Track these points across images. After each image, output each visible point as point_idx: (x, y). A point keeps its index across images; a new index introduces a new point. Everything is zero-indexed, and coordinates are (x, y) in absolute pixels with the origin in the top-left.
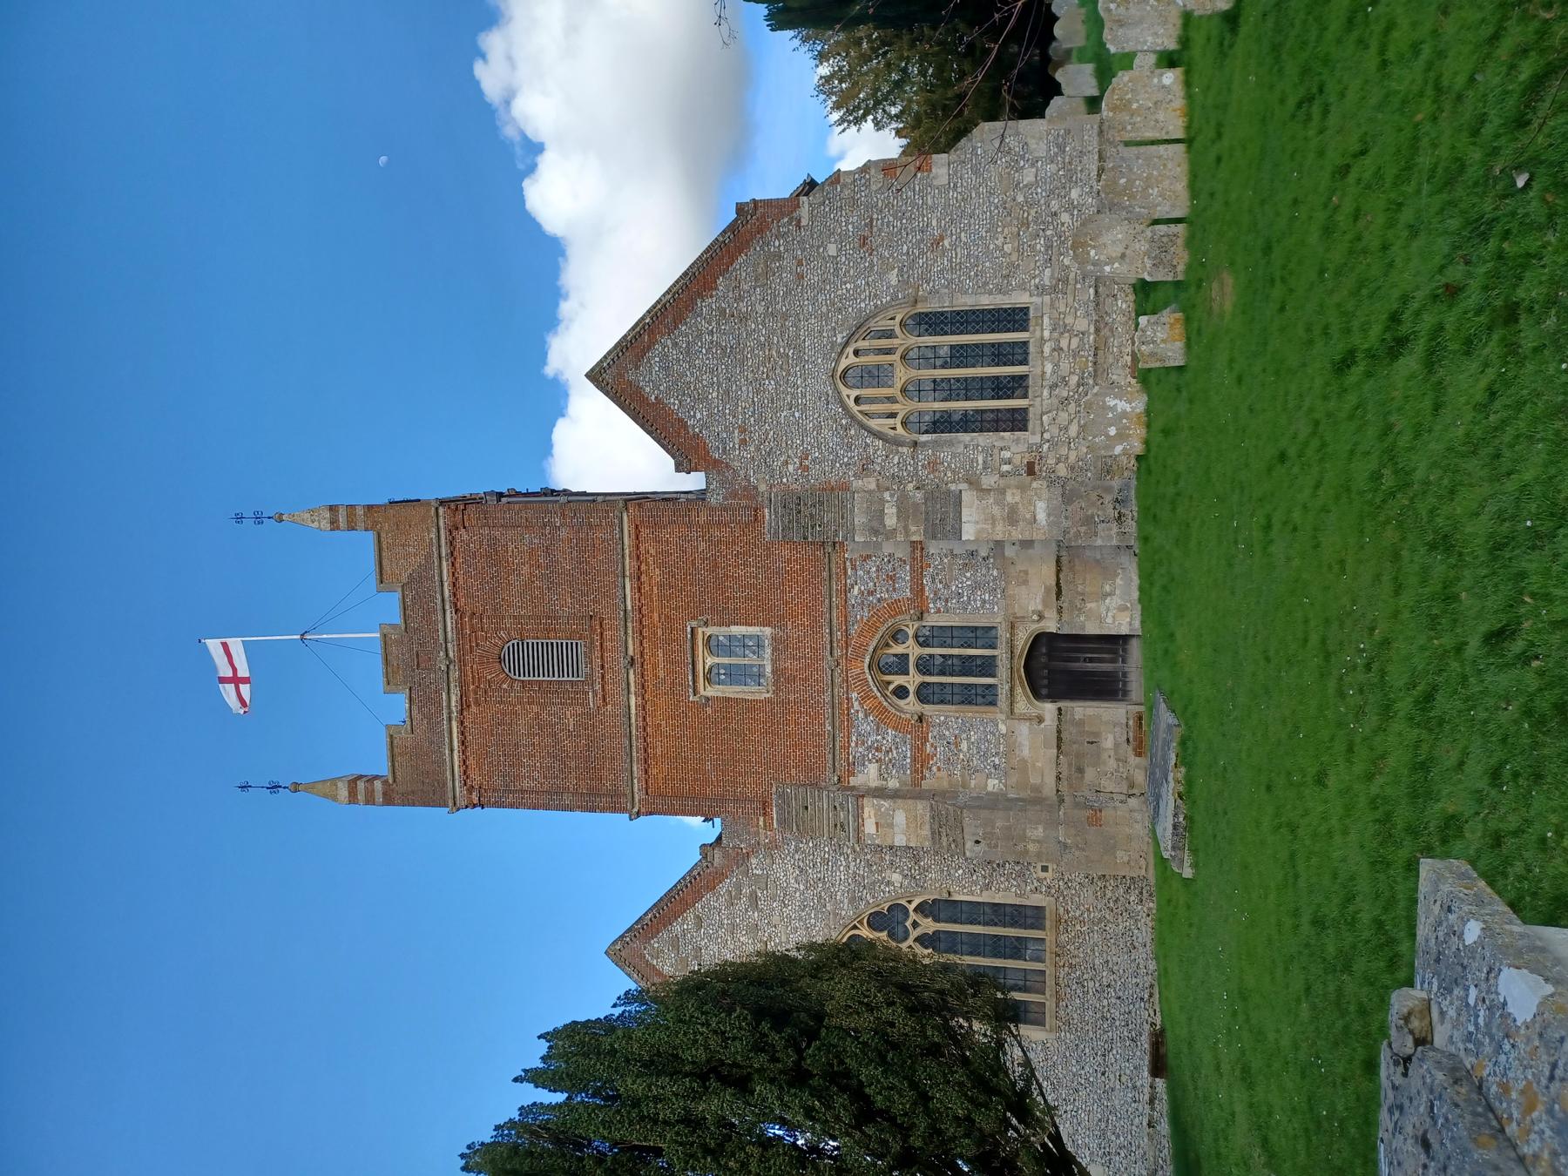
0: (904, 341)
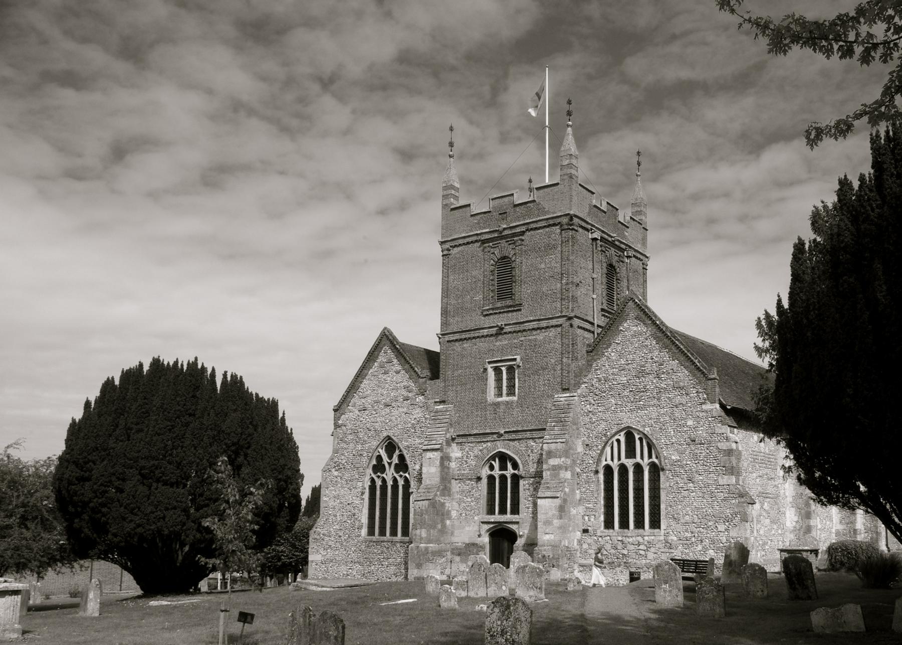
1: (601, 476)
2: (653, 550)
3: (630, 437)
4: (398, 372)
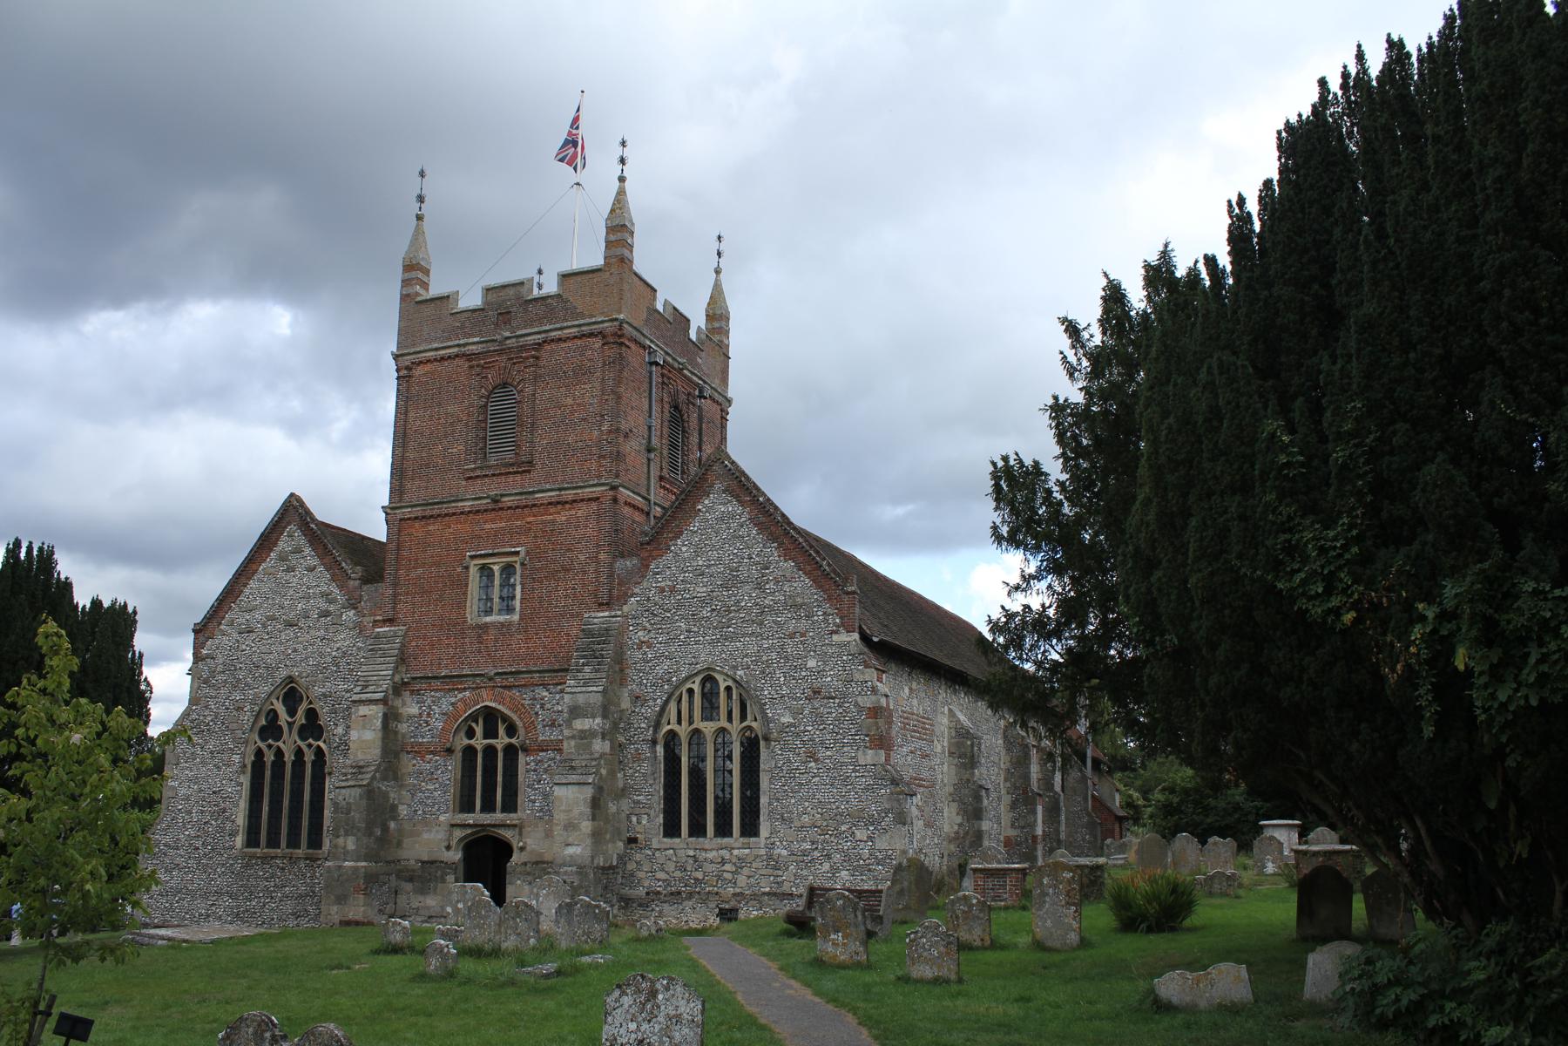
0: (735, 728)
1: (660, 749)
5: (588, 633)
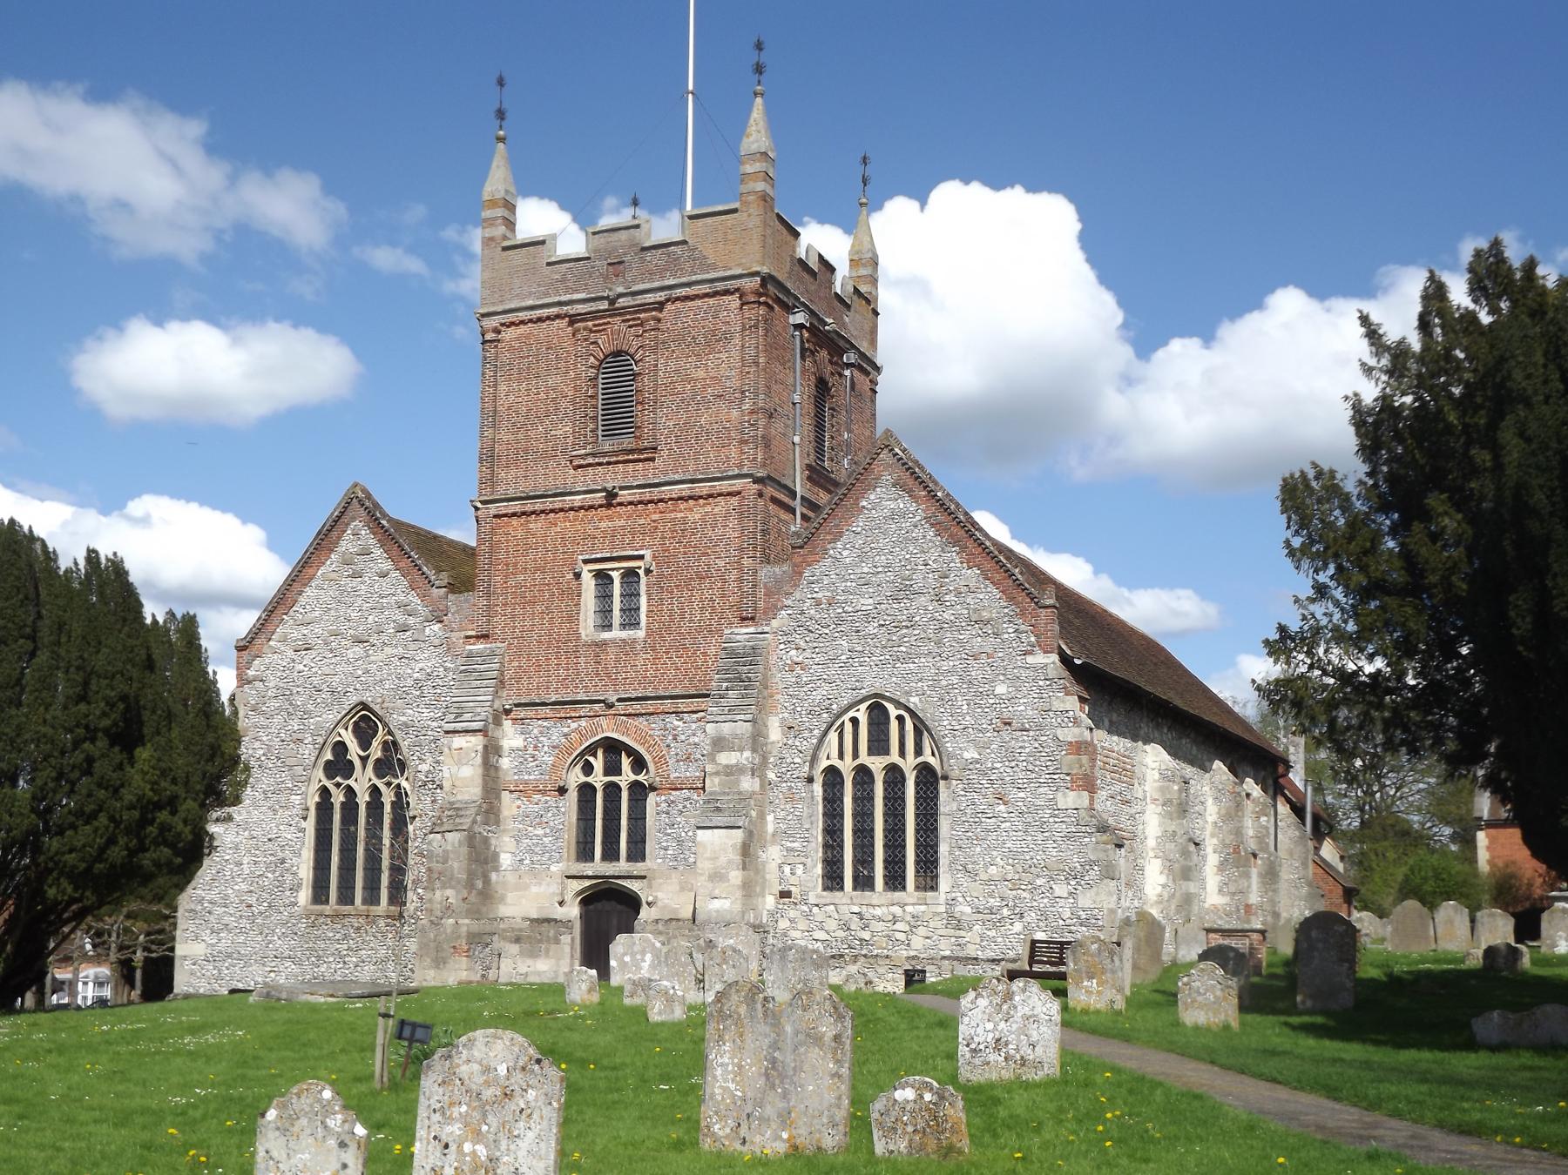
0: (909, 765)
1: (818, 788)
2: (922, 931)
3: (878, 714)
4: (384, 575)
5: (732, 653)
